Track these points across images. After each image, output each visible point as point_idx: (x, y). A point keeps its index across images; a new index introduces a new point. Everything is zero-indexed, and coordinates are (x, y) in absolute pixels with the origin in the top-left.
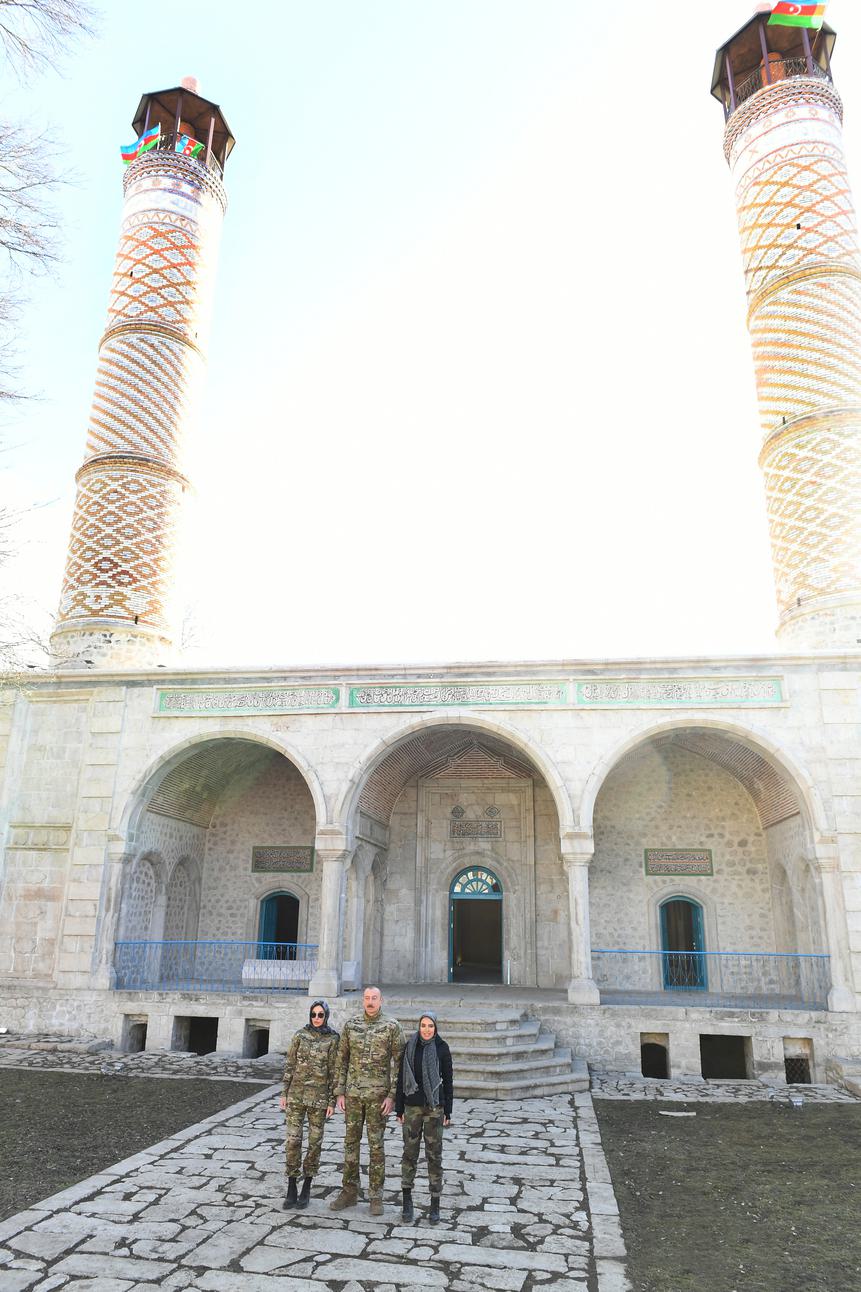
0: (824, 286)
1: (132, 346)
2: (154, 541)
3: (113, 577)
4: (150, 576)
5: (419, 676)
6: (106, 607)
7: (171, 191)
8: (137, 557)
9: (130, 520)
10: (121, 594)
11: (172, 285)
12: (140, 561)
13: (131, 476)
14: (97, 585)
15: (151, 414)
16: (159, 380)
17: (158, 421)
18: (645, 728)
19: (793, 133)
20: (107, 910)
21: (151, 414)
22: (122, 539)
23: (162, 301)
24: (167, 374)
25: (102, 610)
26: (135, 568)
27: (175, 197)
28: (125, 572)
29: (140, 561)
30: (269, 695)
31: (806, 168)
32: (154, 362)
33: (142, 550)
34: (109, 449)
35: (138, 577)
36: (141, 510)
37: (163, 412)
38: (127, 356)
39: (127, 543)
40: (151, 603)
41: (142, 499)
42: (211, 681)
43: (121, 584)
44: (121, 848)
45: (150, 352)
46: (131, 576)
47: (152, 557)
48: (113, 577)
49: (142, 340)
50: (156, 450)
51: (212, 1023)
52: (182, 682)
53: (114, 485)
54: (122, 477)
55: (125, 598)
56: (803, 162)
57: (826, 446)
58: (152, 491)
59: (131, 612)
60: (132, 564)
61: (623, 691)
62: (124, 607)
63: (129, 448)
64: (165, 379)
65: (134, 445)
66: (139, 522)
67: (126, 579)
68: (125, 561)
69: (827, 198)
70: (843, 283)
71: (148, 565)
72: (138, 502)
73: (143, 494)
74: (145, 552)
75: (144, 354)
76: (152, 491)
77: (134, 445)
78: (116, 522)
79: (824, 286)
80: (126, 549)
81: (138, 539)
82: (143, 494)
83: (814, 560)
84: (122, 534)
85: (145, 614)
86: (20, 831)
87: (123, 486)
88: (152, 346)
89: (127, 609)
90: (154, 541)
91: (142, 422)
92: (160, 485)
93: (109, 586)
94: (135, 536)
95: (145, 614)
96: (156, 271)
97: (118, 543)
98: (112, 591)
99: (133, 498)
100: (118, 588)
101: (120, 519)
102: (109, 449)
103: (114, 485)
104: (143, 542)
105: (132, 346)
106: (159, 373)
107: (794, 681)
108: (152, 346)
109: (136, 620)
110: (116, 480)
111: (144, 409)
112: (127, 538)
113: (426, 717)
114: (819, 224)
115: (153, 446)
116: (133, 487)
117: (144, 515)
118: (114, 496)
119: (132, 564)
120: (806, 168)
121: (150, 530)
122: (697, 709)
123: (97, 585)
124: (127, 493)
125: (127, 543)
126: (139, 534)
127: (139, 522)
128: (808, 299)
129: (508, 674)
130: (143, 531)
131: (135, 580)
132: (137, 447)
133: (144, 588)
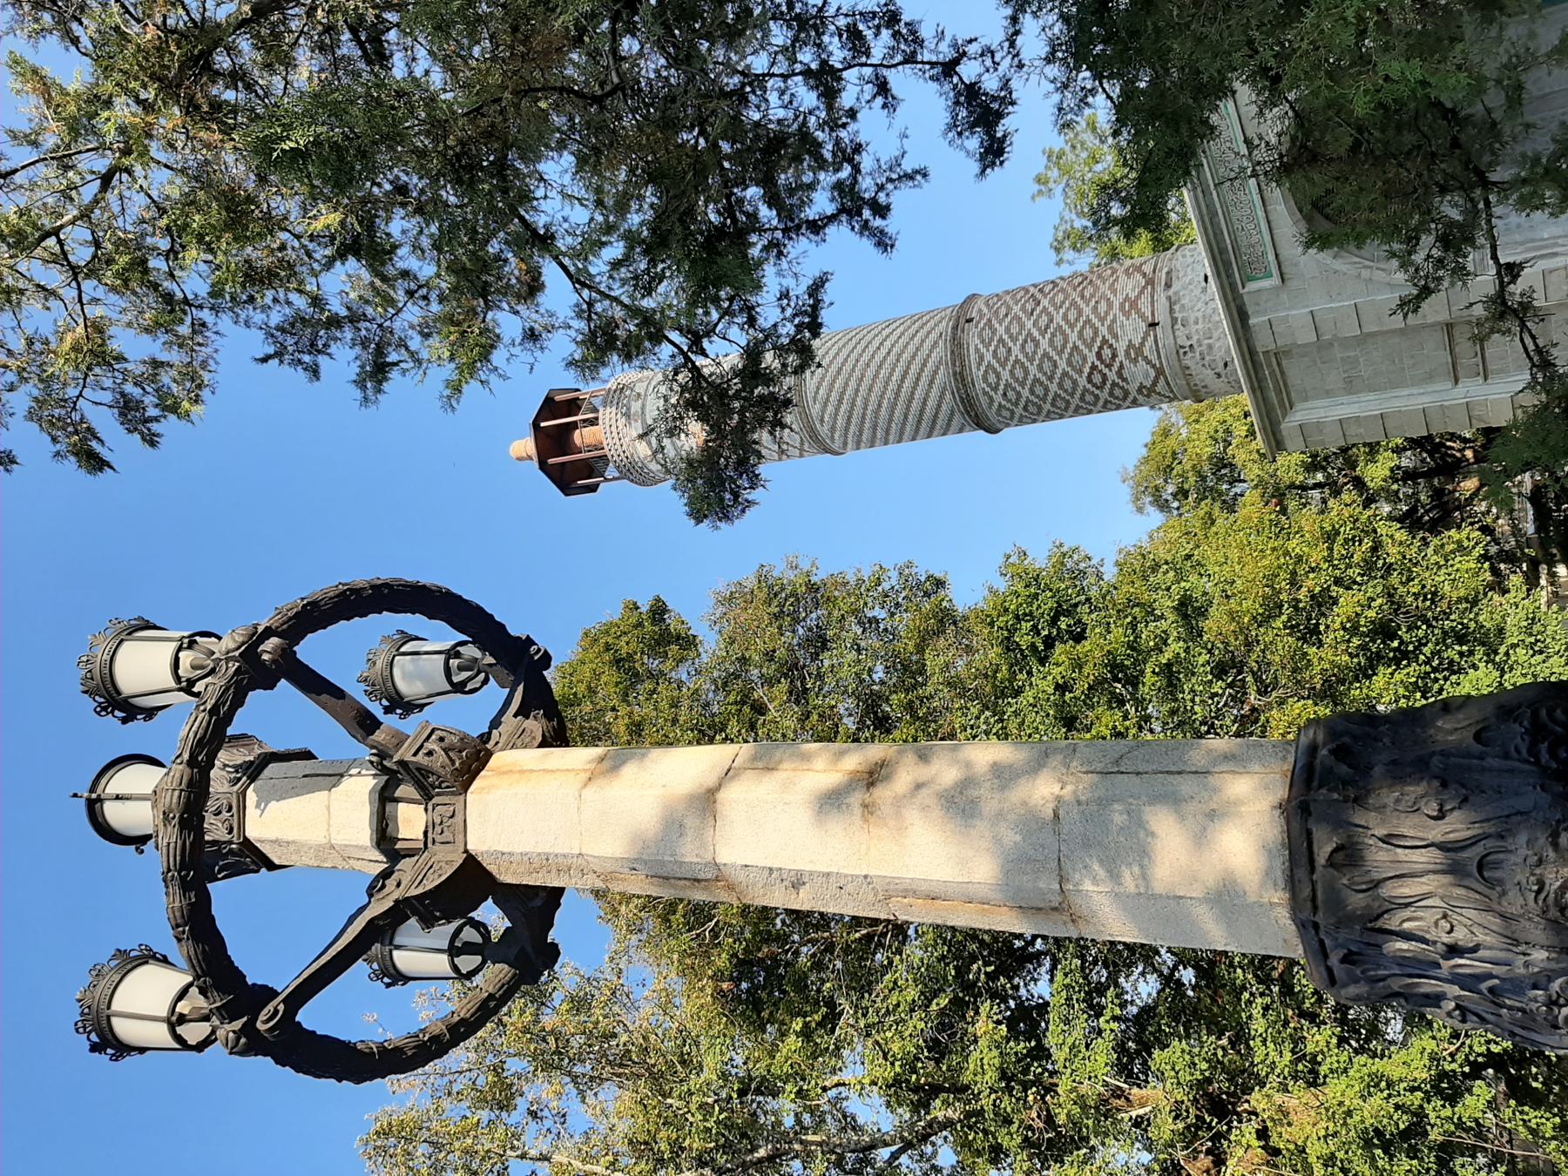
1: (833, 429)
2: (1048, 336)
3: (1109, 366)
4: (1093, 326)
6: (1149, 362)
8: (1075, 347)
9: (1033, 370)
10: (1127, 353)
12: (1079, 343)
13: (980, 385)
14: (1124, 380)
15: (900, 387)
16: (857, 391)
17: (904, 377)
20: (1555, 254)
21: (900, 387)
22: (1059, 372)
24: (846, 384)
25: (1154, 366)
26: (1090, 347)
28: (1099, 355)
29: (1079, 343)
32: (840, 401)
33: (1064, 346)
34: (957, 416)
35: (1099, 339)
36: (1017, 361)
37: (891, 374)
38: (847, 429)
39: (1062, 365)
40: (1127, 315)
41: (1003, 365)
42: (1218, 234)
43: (1114, 356)
45: (830, 408)
46: (1101, 348)
47: (1068, 331)
48: (1109, 366)
49: (822, 421)
50: (938, 368)
52: (1227, 265)
53: (998, 398)
54: (985, 393)
55: (1130, 345)
58: (988, 357)
59: (1147, 334)
60: (1086, 351)
62: (1142, 344)
63: (948, 396)
64: (852, 384)
65: (941, 397)
66: (1031, 360)
67: (1107, 352)
68: (1085, 359)
71: (1081, 333)
72: (1008, 367)
73: (996, 365)
74: (1066, 341)
75: (836, 414)
76: (988, 357)
77: (943, 393)
78: (1041, 384)
80: (1069, 363)
81: (1053, 354)
82: (996, 365)
84: (1053, 372)
85: (1142, 316)
86: (1461, 372)
87: (995, 389)
89: (1144, 339)
90: (1048, 336)
91: (913, 393)
92: (977, 350)
93: (1121, 366)
94: (1050, 359)
95: (1142, 316)
97: (1065, 374)
98: (1126, 363)
99: (1005, 375)
100: (1121, 356)
101: (1036, 380)
102: (957, 416)
103: (998, 398)
104: (1055, 349)
105: (833, 429)
106: (850, 392)
109: (1153, 325)
110: (991, 398)
111: (897, 395)
112: (1055, 365)
115: (936, 372)
116: (992, 378)
117: (1021, 357)
118: (1011, 394)
119: (1086, 351)
121: (1037, 344)
123: (1124, 380)
124: (1002, 383)
125: (1062, 365)
126: (1046, 355)
127: (1031, 360)
130: (1040, 352)
131: (1105, 341)
132: (944, 389)
133: (1110, 328)
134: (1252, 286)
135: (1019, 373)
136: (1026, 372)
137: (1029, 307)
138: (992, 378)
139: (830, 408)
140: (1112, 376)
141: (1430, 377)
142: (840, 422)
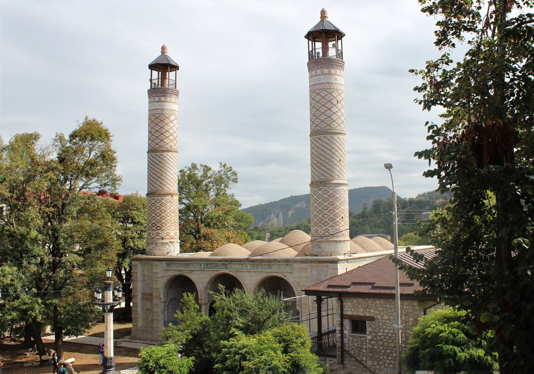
5: (218, 261)
7: (158, 102)
13: (157, 198)
18: (263, 276)
23: (159, 141)
27: (159, 103)
28: (158, 226)
30: (188, 265)
45: (158, 158)
53: (153, 201)
55: (159, 233)
61: (259, 267)
67: (159, 228)
70: (324, 137)
79: (319, 139)
87: (155, 201)
88: (158, 156)
99: (158, 205)
101: (156, 211)
103: (153, 201)
107: (296, 265)
108: (158, 156)
113: (219, 272)
114: (320, 116)
116: (158, 201)
122: (275, 271)
129: (236, 262)
134: (165, 264)
135: (158, 208)
136: (158, 210)
137: (172, 211)
138: (158, 201)
140: (154, 228)
141: (143, 290)
142: (155, 160)
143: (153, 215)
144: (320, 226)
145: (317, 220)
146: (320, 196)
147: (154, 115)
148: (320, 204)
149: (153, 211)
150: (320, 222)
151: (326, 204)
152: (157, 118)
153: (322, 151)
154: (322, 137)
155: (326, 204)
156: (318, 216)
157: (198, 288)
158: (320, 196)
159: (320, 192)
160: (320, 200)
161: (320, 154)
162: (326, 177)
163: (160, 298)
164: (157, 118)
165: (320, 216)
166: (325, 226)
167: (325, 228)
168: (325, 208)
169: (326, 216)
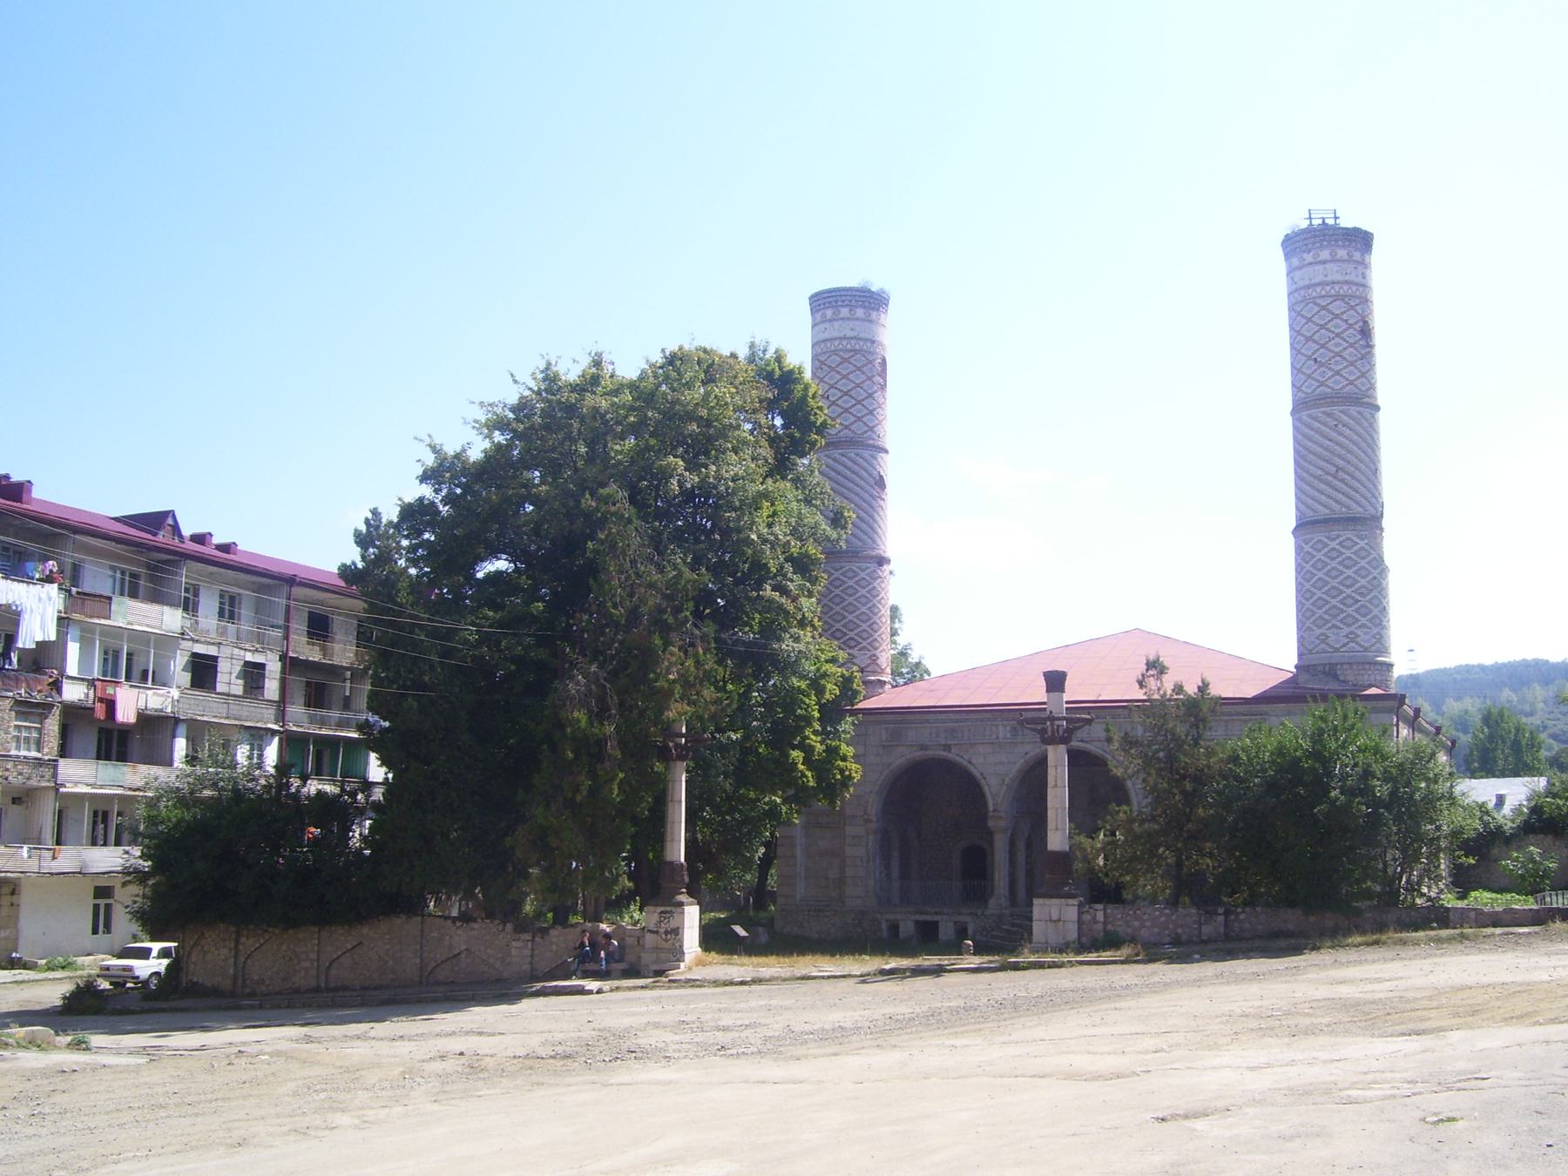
0: (1328, 415)
1: (835, 460)
11: (859, 402)
19: (1317, 273)
27: (851, 324)
31: (1324, 308)
44: (874, 826)
45: (850, 464)
51: (935, 925)
56: (1323, 303)
57: (1319, 546)
64: (862, 483)
69: (1338, 335)
79: (1328, 415)
83: (1309, 628)
96: (846, 394)
105: (835, 460)
120: (1324, 308)
128: (1317, 425)
139: (850, 464)
142: (840, 468)
143: (838, 609)
144: (1334, 626)
145: (1326, 612)
146: (1334, 554)
147: (835, 352)
148: (1334, 573)
149: (837, 600)
150: (1334, 617)
151: (1349, 572)
152: (845, 360)
153: (1337, 443)
154: (1336, 410)
155: (1349, 572)
156: (1327, 602)
157: (986, 789)
158: (1334, 554)
159: (1333, 544)
160: (1334, 564)
161: (1332, 453)
162: (1348, 508)
163: (868, 821)
164: (845, 360)
165: (1334, 602)
166: (1349, 625)
167: (1346, 630)
168: (1348, 582)
169: (1350, 601)
